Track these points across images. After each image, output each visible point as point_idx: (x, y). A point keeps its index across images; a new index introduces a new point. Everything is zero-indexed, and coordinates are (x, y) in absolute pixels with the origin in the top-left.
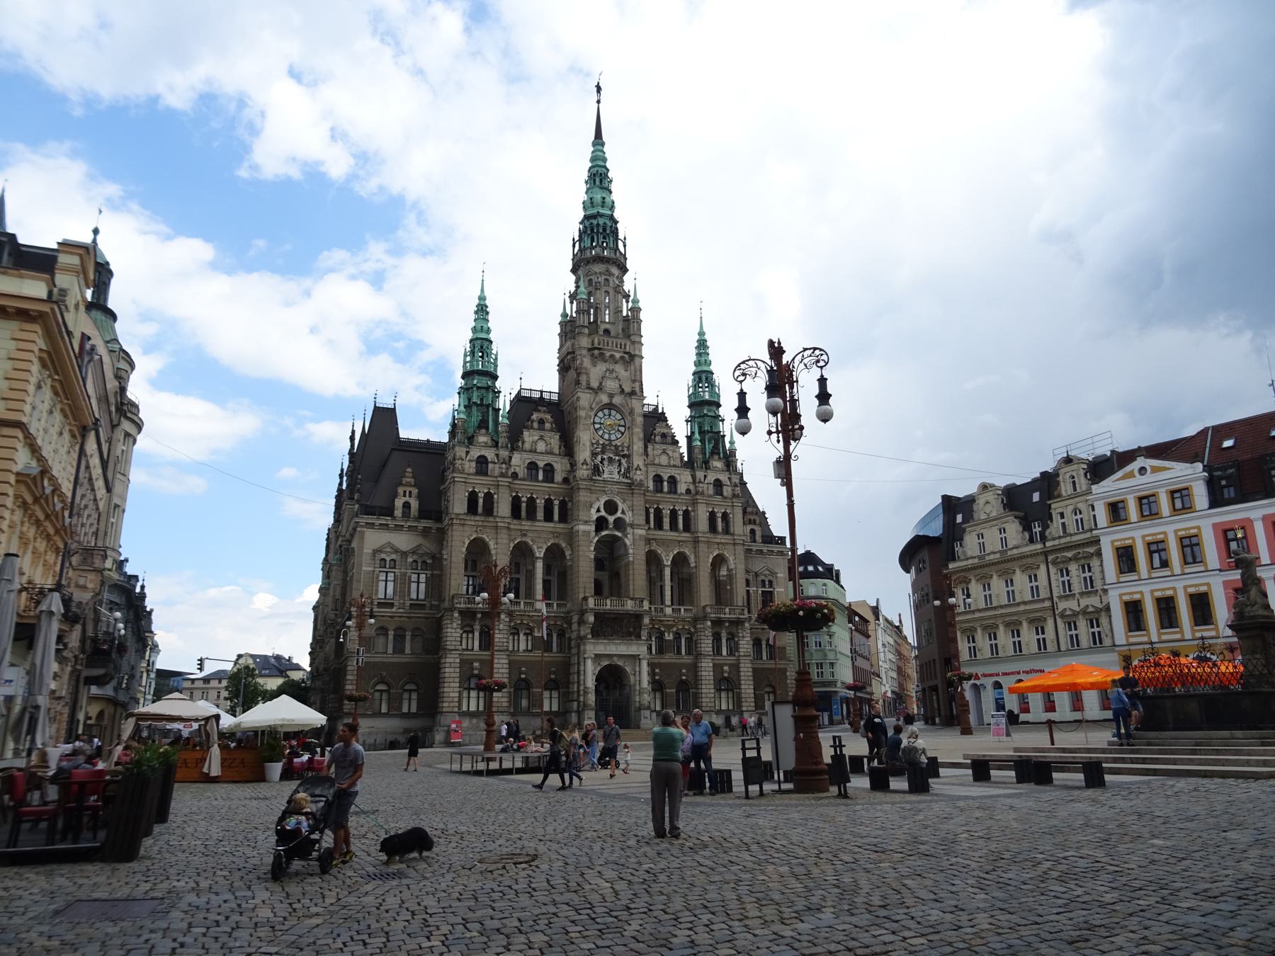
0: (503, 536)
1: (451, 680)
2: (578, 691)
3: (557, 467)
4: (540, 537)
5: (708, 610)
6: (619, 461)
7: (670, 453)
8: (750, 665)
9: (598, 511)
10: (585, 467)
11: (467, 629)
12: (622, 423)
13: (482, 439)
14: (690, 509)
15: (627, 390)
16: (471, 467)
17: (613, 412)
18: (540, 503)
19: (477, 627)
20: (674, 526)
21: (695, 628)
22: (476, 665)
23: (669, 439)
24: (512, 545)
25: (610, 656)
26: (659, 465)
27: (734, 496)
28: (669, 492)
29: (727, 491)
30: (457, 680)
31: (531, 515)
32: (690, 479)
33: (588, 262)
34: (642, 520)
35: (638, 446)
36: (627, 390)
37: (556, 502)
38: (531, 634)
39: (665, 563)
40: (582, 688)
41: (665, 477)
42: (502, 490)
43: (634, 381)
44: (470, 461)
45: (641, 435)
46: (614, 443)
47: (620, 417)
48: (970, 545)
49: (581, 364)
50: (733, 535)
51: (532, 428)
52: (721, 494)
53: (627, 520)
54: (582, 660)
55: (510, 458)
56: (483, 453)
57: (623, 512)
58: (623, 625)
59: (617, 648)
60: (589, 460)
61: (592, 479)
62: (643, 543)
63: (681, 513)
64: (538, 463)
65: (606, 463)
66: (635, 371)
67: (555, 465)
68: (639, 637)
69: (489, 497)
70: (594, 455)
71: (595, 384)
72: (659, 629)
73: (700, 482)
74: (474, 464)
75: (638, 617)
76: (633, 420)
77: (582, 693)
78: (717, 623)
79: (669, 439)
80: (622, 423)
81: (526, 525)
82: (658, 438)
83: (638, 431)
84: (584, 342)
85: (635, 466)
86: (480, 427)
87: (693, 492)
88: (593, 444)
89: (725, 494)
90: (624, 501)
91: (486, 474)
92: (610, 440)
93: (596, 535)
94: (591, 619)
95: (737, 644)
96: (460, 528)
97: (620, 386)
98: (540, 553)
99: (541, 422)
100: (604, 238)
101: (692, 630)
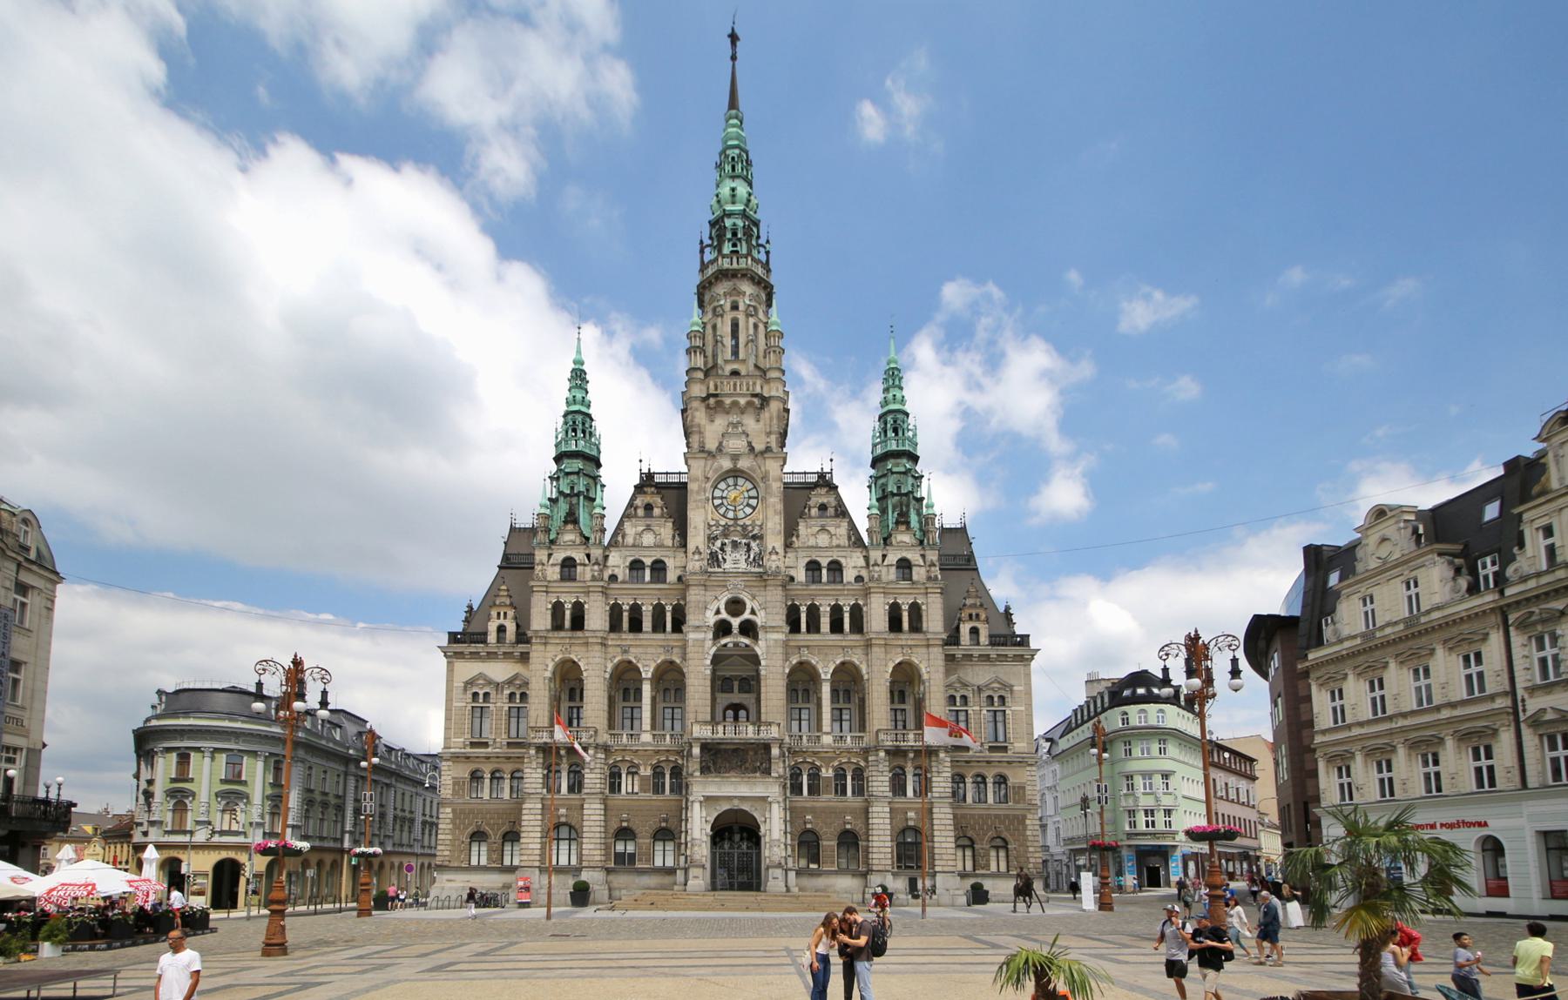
0: (596, 651)
1: (530, 829)
2: (686, 844)
3: (670, 563)
4: (648, 653)
5: (882, 736)
6: (748, 545)
7: (832, 529)
8: (949, 810)
9: (718, 612)
10: (697, 557)
11: (550, 772)
12: (753, 493)
13: (569, 537)
14: (861, 602)
15: (759, 447)
16: (553, 573)
17: (741, 481)
18: (647, 610)
19: (565, 767)
20: (836, 627)
21: (866, 760)
22: (563, 811)
23: (831, 511)
24: (610, 666)
25: (730, 798)
26: (816, 547)
27: (929, 578)
28: (829, 582)
29: (919, 574)
30: (539, 829)
31: (636, 626)
32: (862, 562)
33: (710, 283)
34: (779, 619)
35: (774, 524)
36: (759, 447)
37: (669, 608)
38: (636, 773)
39: (823, 677)
40: (689, 839)
41: (824, 562)
42: (593, 597)
43: (769, 434)
44: (552, 565)
45: (780, 507)
46: (740, 522)
47: (750, 486)
48: (1349, 619)
49: (692, 421)
50: (925, 633)
51: (636, 516)
52: (911, 579)
53: (759, 624)
54: (689, 804)
55: (606, 558)
56: (568, 553)
57: (753, 612)
58: (750, 758)
59: (735, 789)
60: (702, 548)
61: (707, 572)
62: (780, 650)
63: (847, 609)
64: (644, 560)
65: (728, 549)
66: (771, 419)
67: (666, 560)
68: (767, 772)
69: (579, 610)
70: (712, 539)
71: (711, 445)
72: (813, 763)
73: (876, 564)
74: (558, 569)
75: (767, 747)
76: (768, 487)
77: (689, 845)
78: (896, 753)
79: (831, 511)
80: (753, 493)
81: (628, 638)
82: (814, 511)
83: (775, 502)
84: (698, 390)
85: (770, 548)
86: (566, 522)
87: (866, 580)
88: (710, 526)
89: (915, 577)
90: (754, 597)
91: (574, 580)
92: (736, 519)
93: (714, 644)
94: (696, 751)
95: (928, 781)
96: (542, 648)
97: (750, 444)
98: (647, 672)
99: (649, 508)
100: (734, 245)
101: (862, 764)
